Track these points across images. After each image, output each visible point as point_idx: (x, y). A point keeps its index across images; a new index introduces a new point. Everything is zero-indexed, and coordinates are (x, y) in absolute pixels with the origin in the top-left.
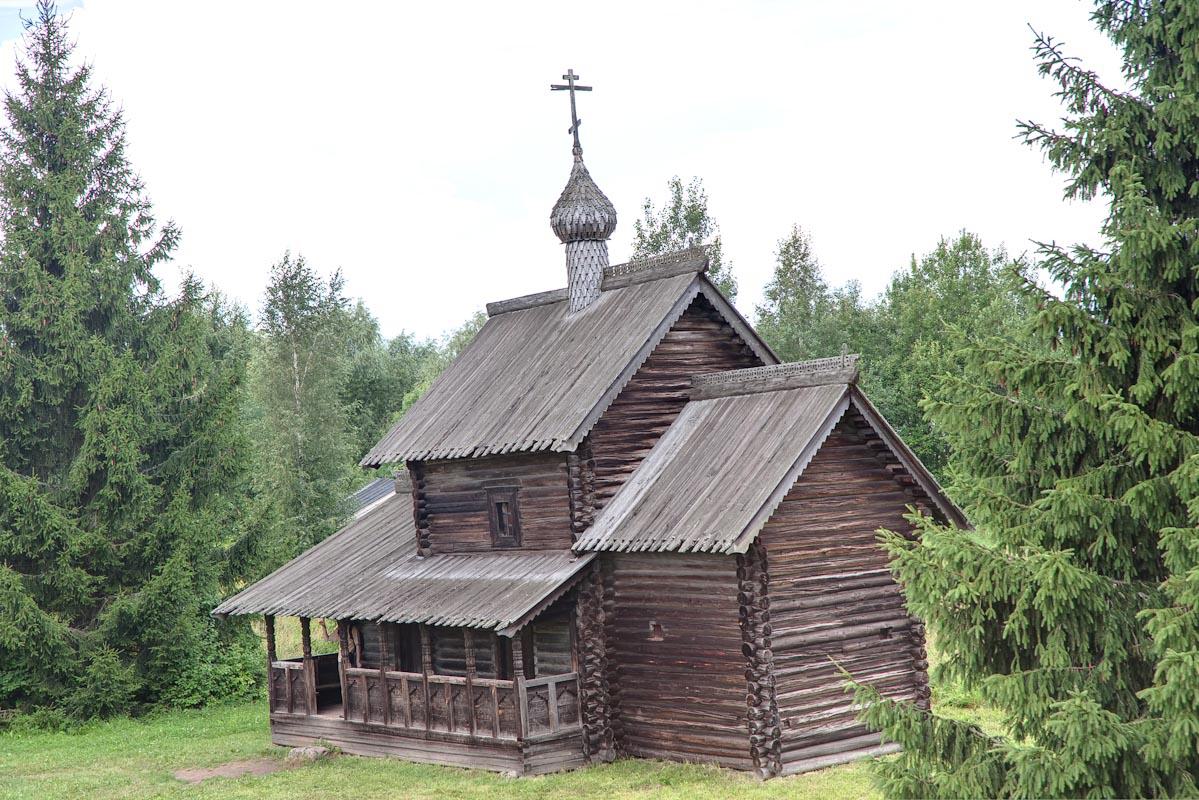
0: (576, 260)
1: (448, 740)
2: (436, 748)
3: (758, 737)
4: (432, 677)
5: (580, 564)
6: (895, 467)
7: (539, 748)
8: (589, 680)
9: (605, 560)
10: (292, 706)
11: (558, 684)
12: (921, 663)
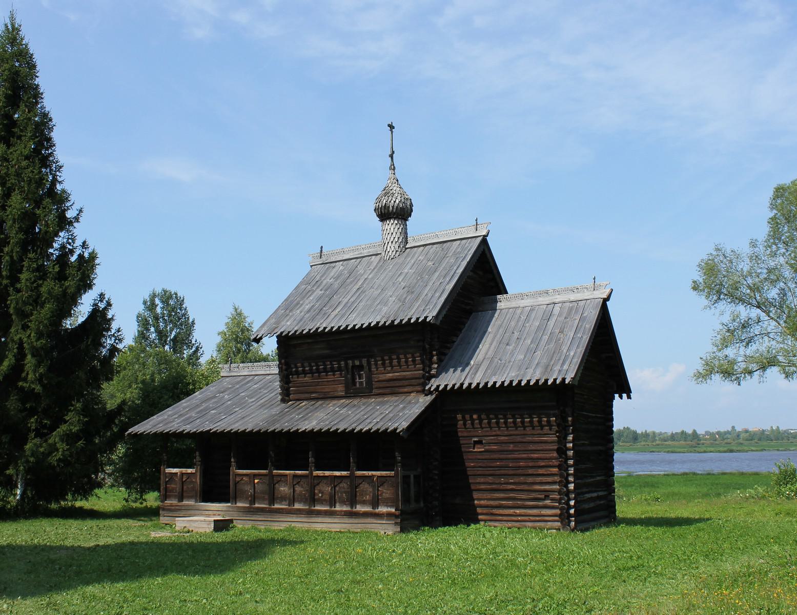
4: (316, 473)
5: (429, 398)
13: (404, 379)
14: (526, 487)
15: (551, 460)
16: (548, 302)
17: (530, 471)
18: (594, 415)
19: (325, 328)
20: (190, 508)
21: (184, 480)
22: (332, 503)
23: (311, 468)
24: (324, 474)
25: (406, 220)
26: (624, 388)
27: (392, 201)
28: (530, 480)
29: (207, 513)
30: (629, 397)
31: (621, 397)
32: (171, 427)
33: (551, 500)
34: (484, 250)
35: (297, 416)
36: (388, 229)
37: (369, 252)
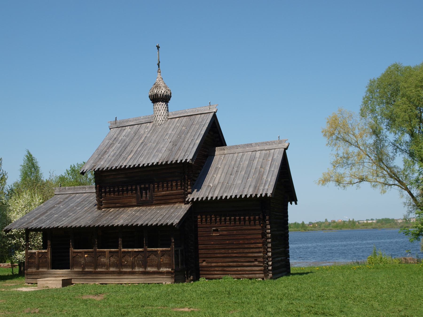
0: (160, 107)
1: (132, 273)
4: (123, 250)
5: (188, 206)
13: (173, 195)
14: (244, 255)
15: (257, 240)
16: (252, 150)
17: (246, 246)
18: (279, 214)
19: (125, 166)
20: (45, 273)
21: (40, 256)
22: (133, 267)
23: (120, 247)
24: (128, 250)
25: (168, 102)
26: (293, 198)
27: (160, 91)
28: (246, 251)
29: (55, 275)
30: (296, 204)
31: (291, 204)
32: (32, 225)
33: (258, 262)
34: (214, 120)
35: (110, 217)
36: (158, 108)
37: (146, 121)
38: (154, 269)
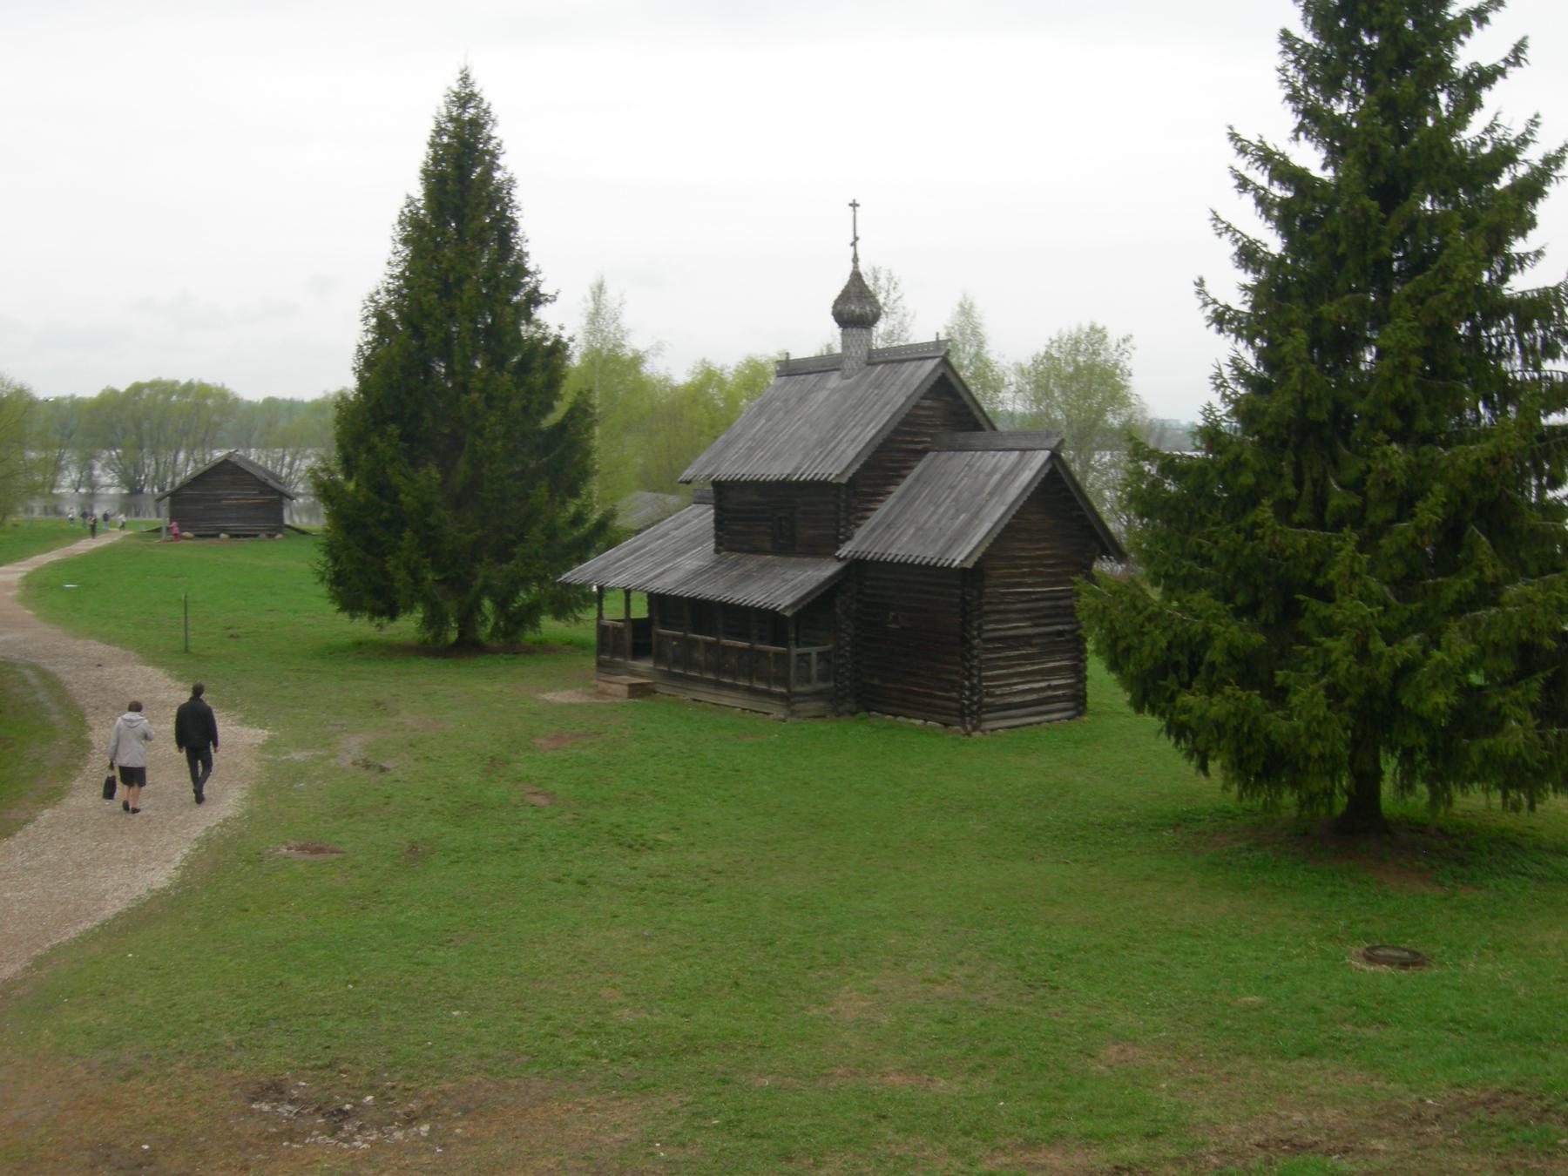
1: (733, 687)
2: (725, 692)
3: (966, 702)
6: (1080, 513)
7: (801, 699)
8: (842, 652)
9: (858, 568)
10: (614, 653)
11: (819, 653)
12: (1083, 657)
34: (943, 375)
38: (763, 686)
